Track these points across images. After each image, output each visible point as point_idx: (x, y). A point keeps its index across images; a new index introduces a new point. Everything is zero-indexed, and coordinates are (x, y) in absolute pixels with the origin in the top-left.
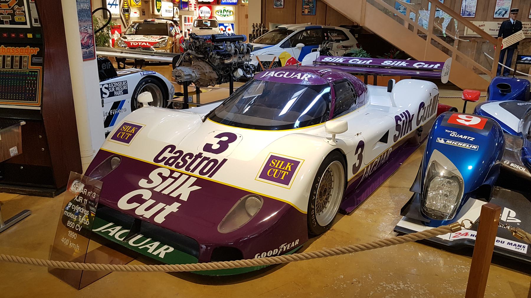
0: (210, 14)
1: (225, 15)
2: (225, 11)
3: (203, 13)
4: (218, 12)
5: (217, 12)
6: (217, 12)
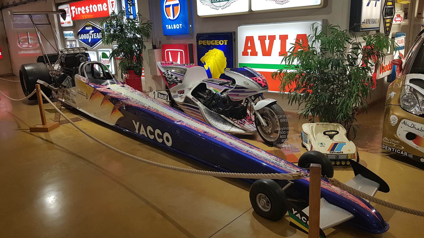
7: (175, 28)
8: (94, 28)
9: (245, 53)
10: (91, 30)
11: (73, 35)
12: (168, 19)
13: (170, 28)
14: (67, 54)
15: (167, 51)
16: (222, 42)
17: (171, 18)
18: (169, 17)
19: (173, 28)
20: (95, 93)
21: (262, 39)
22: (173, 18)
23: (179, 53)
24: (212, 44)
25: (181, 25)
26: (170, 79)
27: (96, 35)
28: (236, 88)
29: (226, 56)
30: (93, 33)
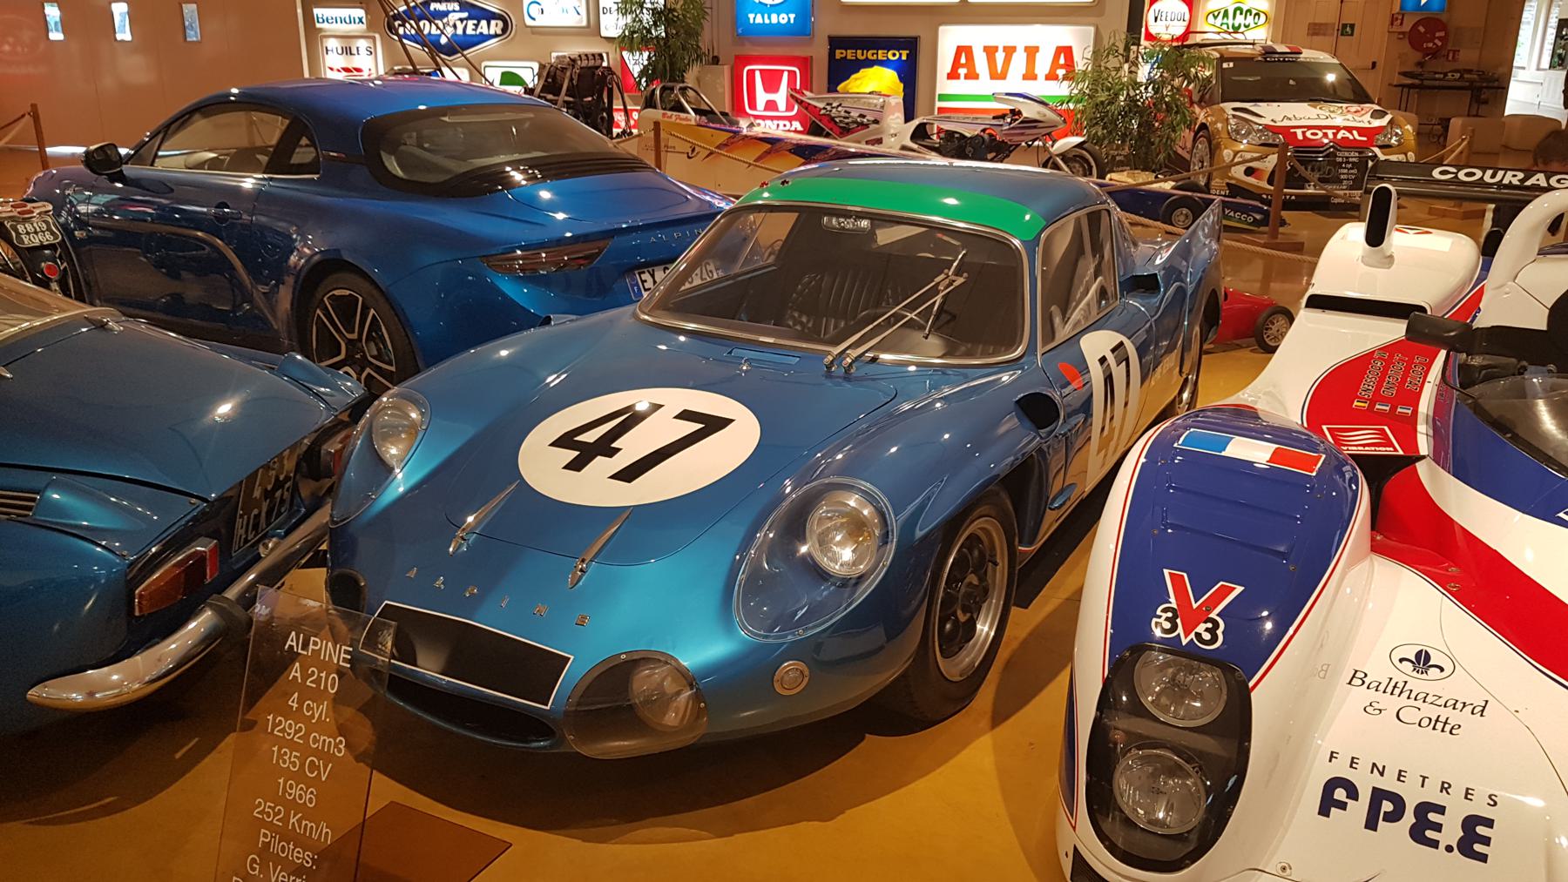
0: (1186, 24)
1: (1236, 25)
2: (1241, 14)
3: (1163, 18)
4: (1215, 17)
5: (1211, 16)
6: (1211, 16)
7: (767, 21)
8: (465, 7)
9: (953, 75)
10: (454, 11)
11: (364, 20)
13: (759, 20)
14: (581, 68)
15: (748, 70)
16: (894, 55)
20: (732, 143)
21: (990, 51)
23: (786, 74)
24: (870, 57)
25: (792, 16)
26: (845, 118)
27: (477, 26)
28: (1022, 122)
29: (901, 79)
30: (461, 20)
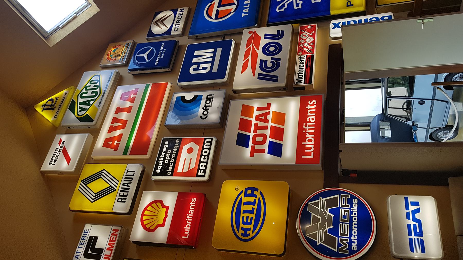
12: (234, 13)
13: (246, 11)
17: (234, 7)
18: (232, 11)
19: (249, 4)
22: (236, 4)
